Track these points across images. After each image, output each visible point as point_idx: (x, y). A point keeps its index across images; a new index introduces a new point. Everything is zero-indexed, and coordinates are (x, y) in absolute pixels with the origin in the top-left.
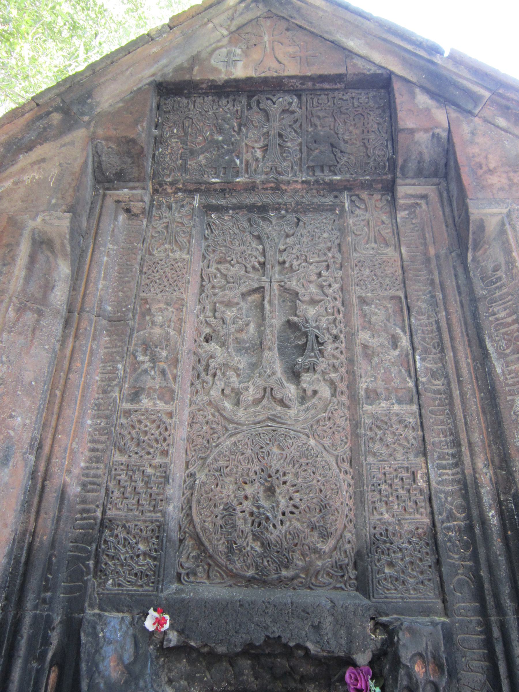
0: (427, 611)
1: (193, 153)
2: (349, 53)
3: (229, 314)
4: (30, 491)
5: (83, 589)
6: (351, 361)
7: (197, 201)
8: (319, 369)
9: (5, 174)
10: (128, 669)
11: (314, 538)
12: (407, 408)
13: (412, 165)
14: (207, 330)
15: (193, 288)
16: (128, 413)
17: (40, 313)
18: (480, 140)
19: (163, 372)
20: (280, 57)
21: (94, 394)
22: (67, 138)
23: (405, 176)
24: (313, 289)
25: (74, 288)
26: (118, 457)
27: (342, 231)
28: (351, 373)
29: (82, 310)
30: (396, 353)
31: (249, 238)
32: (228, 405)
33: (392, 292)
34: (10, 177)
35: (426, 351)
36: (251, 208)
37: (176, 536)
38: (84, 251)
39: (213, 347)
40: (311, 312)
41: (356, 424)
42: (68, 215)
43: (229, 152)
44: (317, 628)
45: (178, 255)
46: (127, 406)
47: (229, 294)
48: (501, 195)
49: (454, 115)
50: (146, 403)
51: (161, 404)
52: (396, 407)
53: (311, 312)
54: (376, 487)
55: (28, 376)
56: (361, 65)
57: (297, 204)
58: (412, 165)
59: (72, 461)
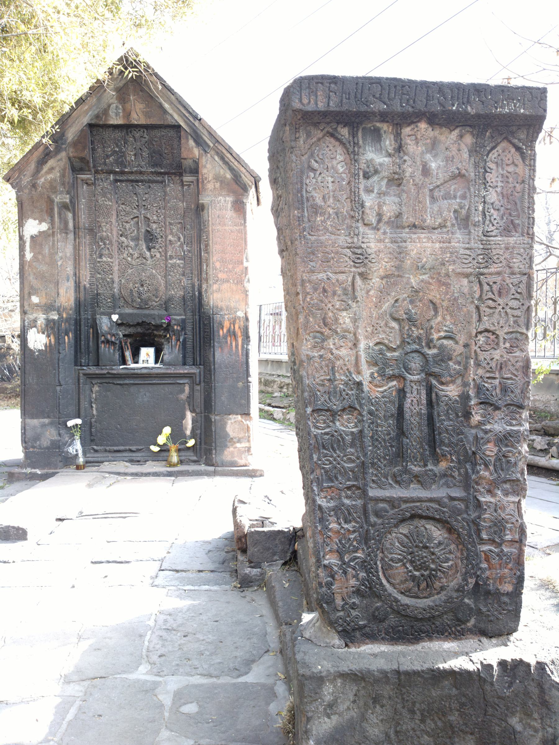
0: (181, 315)
1: (108, 157)
2: (165, 111)
3: (128, 226)
4: (76, 287)
5: (95, 311)
6: (166, 246)
7: (112, 177)
8: (157, 247)
9: (40, 175)
10: (109, 328)
11: (154, 298)
12: (181, 261)
13: (188, 170)
14: (121, 233)
15: (114, 217)
16: (99, 262)
17: (67, 233)
18: (208, 166)
19: (108, 249)
20: (138, 111)
21: (88, 257)
22: (59, 157)
23: (186, 173)
24: (155, 218)
25: (74, 220)
26: (99, 276)
27: (165, 192)
28: (166, 250)
29: (78, 228)
30: (179, 243)
31: (133, 195)
32: (129, 259)
33: (180, 221)
34: (42, 176)
35: (188, 243)
36: (132, 181)
37: (118, 297)
38: (75, 204)
39: (123, 239)
40: (154, 226)
41: (166, 267)
42: (68, 196)
43: (122, 156)
44: (154, 319)
45: (107, 203)
46: (98, 260)
47: (127, 219)
48: (211, 193)
49: (202, 152)
50: (104, 259)
51: (109, 259)
52: (178, 261)
53: (154, 226)
54: (170, 285)
55: (68, 255)
56: (170, 121)
57: (149, 180)
58: (188, 170)
59: (86, 278)
